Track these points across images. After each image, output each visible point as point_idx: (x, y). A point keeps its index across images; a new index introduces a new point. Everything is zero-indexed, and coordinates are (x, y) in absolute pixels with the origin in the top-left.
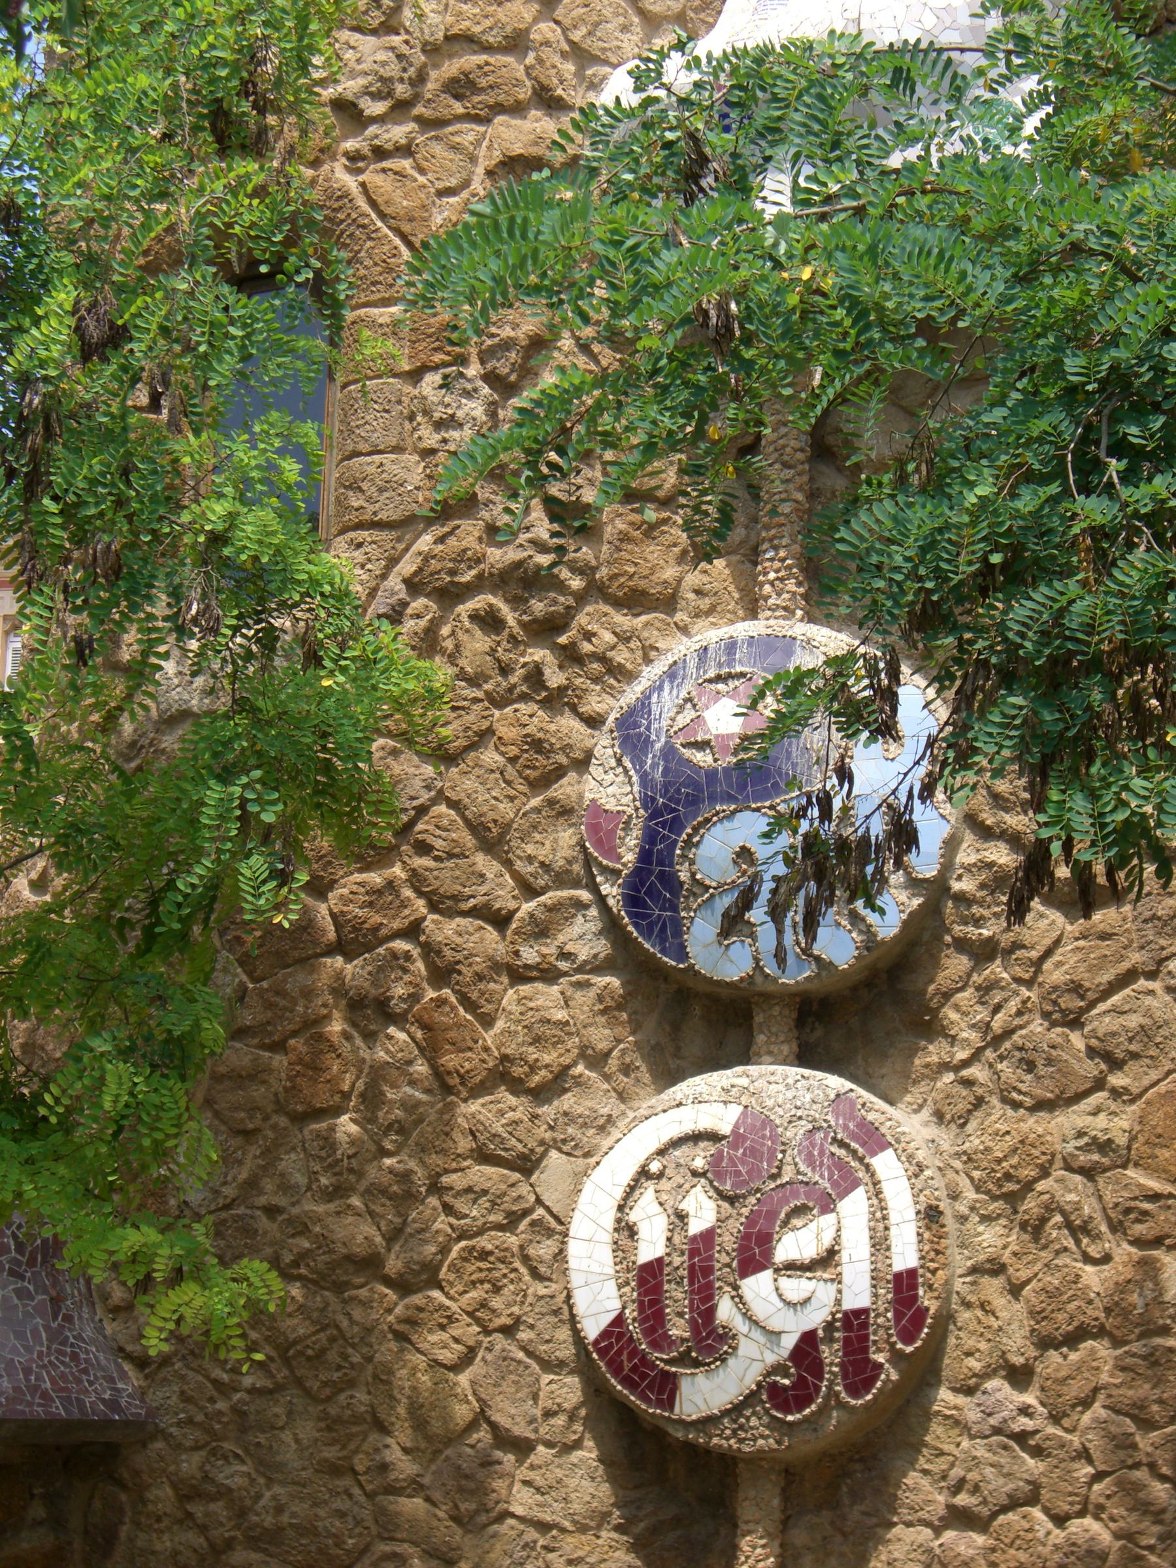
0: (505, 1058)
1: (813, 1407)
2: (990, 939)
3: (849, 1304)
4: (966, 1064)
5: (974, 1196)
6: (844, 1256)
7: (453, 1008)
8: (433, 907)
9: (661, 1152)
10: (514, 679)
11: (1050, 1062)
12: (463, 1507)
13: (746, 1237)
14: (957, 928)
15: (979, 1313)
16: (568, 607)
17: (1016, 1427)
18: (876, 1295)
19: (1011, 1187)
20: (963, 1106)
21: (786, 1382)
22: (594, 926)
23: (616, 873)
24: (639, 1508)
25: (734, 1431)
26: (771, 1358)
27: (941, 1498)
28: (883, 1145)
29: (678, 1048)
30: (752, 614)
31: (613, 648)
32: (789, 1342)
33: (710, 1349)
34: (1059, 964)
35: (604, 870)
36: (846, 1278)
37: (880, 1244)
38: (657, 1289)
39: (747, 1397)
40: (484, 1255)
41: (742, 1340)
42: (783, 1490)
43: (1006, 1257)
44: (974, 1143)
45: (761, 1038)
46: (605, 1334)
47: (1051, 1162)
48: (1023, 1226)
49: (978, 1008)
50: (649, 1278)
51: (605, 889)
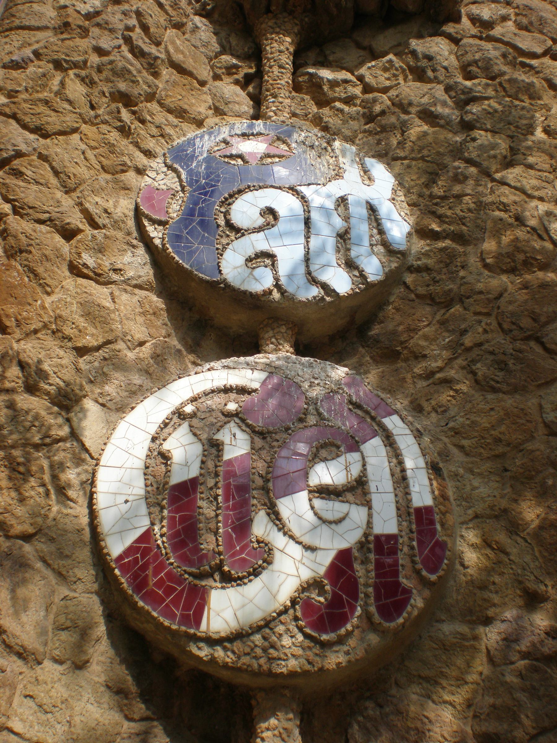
0: (58, 317)
1: (349, 627)
4: (441, 369)
8: (15, 211)
9: (194, 400)
10: (100, 112)
18: (400, 524)
19: (500, 449)
21: (322, 599)
25: (265, 650)
32: (326, 559)
35: (154, 222)
36: (375, 504)
37: (401, 479)
38: (191, 505)
39: (280, 614)
41: (277, 555)
46: (129, 551)
49: (446, 334)
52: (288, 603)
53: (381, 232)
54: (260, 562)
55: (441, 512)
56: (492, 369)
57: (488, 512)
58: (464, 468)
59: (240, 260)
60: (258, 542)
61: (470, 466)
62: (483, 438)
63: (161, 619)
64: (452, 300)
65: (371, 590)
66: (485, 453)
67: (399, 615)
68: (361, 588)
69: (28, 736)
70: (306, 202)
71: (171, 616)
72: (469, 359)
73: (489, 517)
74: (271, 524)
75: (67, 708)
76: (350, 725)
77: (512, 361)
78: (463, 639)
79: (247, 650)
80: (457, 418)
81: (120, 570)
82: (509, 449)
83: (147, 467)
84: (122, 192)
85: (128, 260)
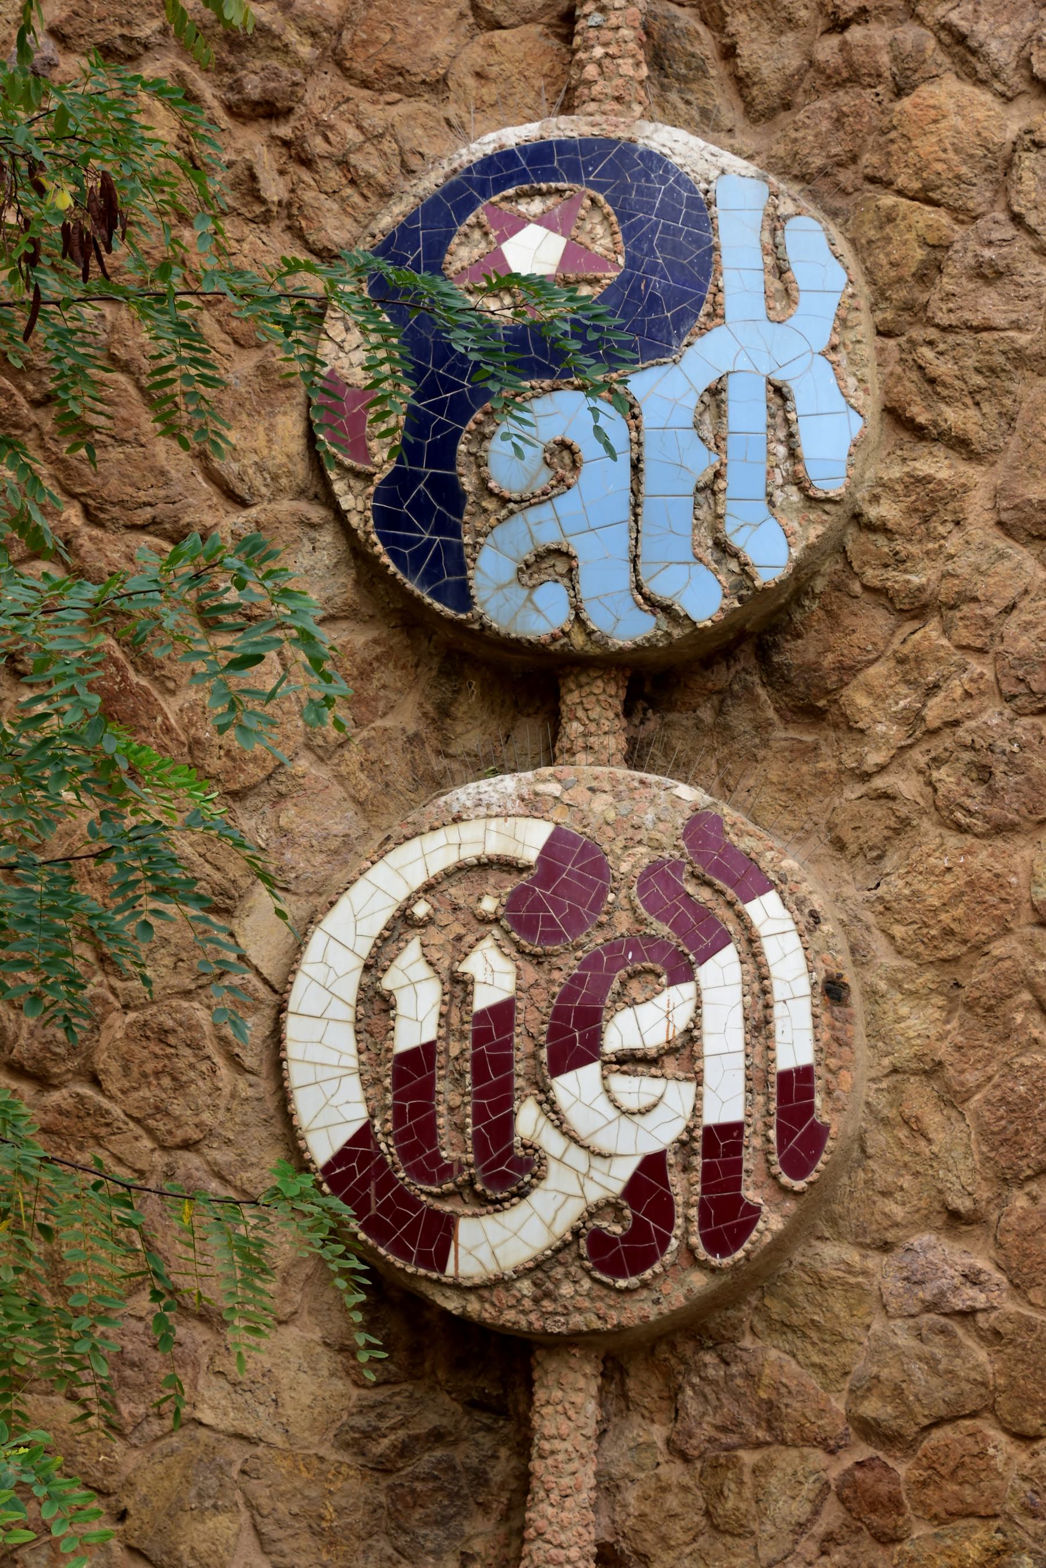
1: (657, 1268)
2: (921, 589)
3: (712, 1117)
4: (882, 769)
5: (897, 962)
6: (710, 1044)
7: (120, 668)
8: (90, 516)
9: (428, 888)
11: (1013, 766)
12: (125, 1409)
13: (559, 1013)
14: (870, 572)
15: (903, 1133)
16: (295, 84)
17: (958, 1303)
18: (749, 1103)
19: (951, 949)
20: (875, 833)
21: (618, 1229)
22: (325, 558)
23: (368, 477)
24: (381, 1416)
25: (536, 1301)
26: (595, 1194)
27: (839, 1405)
28: (765, 886)
29: (446, 741)
30: (567, 109)
31: (360, 149)
32: (624, 1170)
33: (501, 1180)
34: (1027, 627)
36: (708, 1077)
37: (760, 1026)
38: (427, 1090)
39: (557, 1251)
40: (163, 1034)
41: (553, 1166)
42: (600, 1389)
43: (943, 1051)
44: (895, 886)
45: (574, 728)
46: (342, 1157)
47: (1015, 914)
48: (969, 1007)
49: (903, 689)
50: (415, 1069)
51: (346, 502)
52: (569, 1237)
53: (793, 455)
54: (527, 1178)
55: (830, 1071)
56: (965, 780)
57: (914, 1065)
58: (888, 979)
59: (507, 570)
60: (524, 1146)
61: (900, 976)
62: (926, 925)
63: (391, 1258)
64: (925, 606)
65: (694, 1212)
66: (927, 955)
67: (737, 1248)
68: (679, 1210)
69: (222, 1427)
70: (635, 417)
71: (406, 1255)
72: (933, 754)
73: (915, 1073)
74: (543, 1119)
75: (271, 1382)
76: (680, 1388)
77: (1002, 767)
78: (850, 1273)
79: (512, 1302)
80: (893, 878)
81: (330, 1185)
82: (964, 949)
83: (358, 1021)
84: (282, 395)
85: (306, 563)
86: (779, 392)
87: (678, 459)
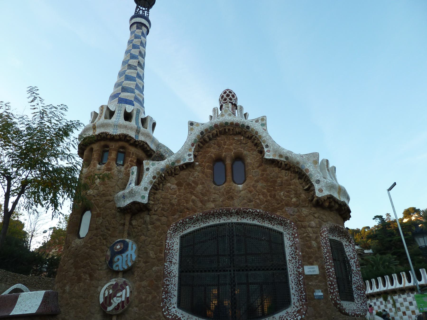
37: (126, 294)
86: (131, 255)
87: (125, 259)
